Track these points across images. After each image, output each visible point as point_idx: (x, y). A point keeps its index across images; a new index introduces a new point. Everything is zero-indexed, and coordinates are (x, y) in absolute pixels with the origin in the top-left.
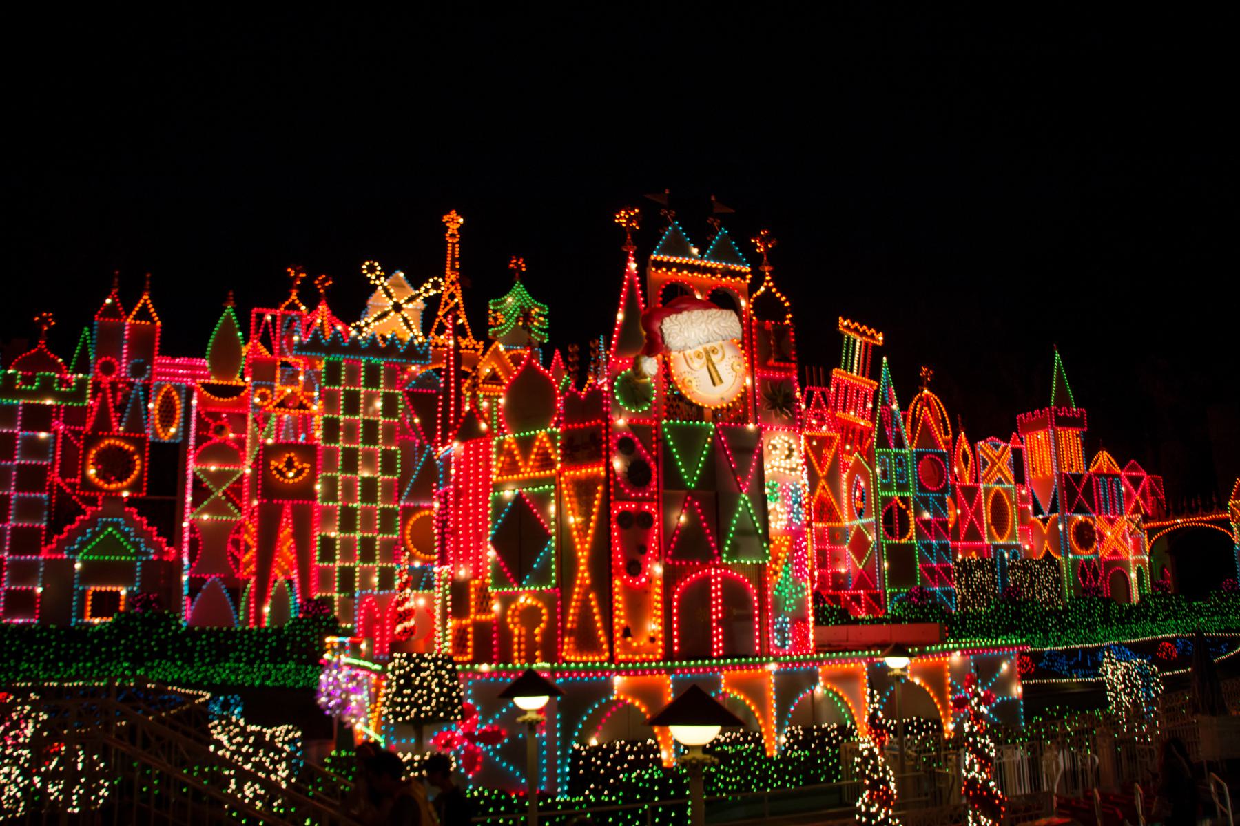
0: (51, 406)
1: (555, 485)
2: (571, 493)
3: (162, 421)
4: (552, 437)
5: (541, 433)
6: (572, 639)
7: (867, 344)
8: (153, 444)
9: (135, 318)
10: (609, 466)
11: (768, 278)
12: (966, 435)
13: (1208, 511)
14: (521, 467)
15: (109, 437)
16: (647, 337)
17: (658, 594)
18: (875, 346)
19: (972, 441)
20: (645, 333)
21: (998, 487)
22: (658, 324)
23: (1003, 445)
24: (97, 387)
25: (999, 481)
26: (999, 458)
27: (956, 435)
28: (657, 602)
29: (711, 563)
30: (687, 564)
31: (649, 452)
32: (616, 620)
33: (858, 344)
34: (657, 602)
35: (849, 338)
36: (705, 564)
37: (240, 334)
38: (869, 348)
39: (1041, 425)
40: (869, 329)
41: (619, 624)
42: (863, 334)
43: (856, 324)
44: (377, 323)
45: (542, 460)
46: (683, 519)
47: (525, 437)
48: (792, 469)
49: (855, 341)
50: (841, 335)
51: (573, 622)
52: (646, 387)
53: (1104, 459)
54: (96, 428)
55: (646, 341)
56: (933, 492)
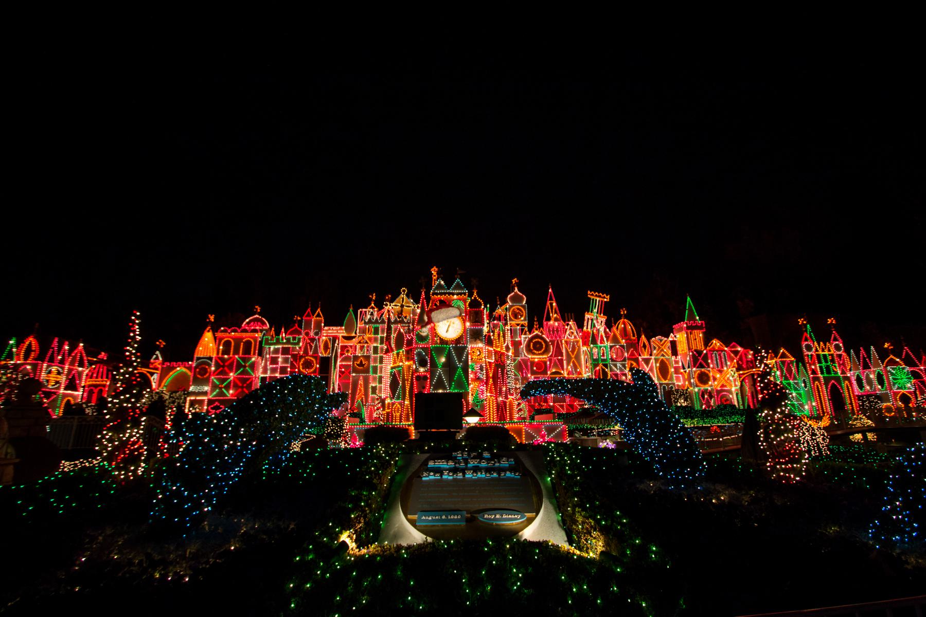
4: (403, 351)
5: (401, 351)
7: (602, 301)
9: (316, 317)
11: (475, 294)
12: (645, 336)
18: (606, 302)
19: (649, 339)
21: (662, 357)
23: (666, 339)
25: (663, 355)
26: (662, 345)
27: (639, 337)
33: (597, 302)
35: (593, 299)
38: (603, 303)
39: (680, 330)
40: (603, 295)
42: (600, 296)
43: (597, 293)
48: (480, 359)
49: (596, 300)
50: (590, 299)
53: (716, 343)
56: (618, 361)
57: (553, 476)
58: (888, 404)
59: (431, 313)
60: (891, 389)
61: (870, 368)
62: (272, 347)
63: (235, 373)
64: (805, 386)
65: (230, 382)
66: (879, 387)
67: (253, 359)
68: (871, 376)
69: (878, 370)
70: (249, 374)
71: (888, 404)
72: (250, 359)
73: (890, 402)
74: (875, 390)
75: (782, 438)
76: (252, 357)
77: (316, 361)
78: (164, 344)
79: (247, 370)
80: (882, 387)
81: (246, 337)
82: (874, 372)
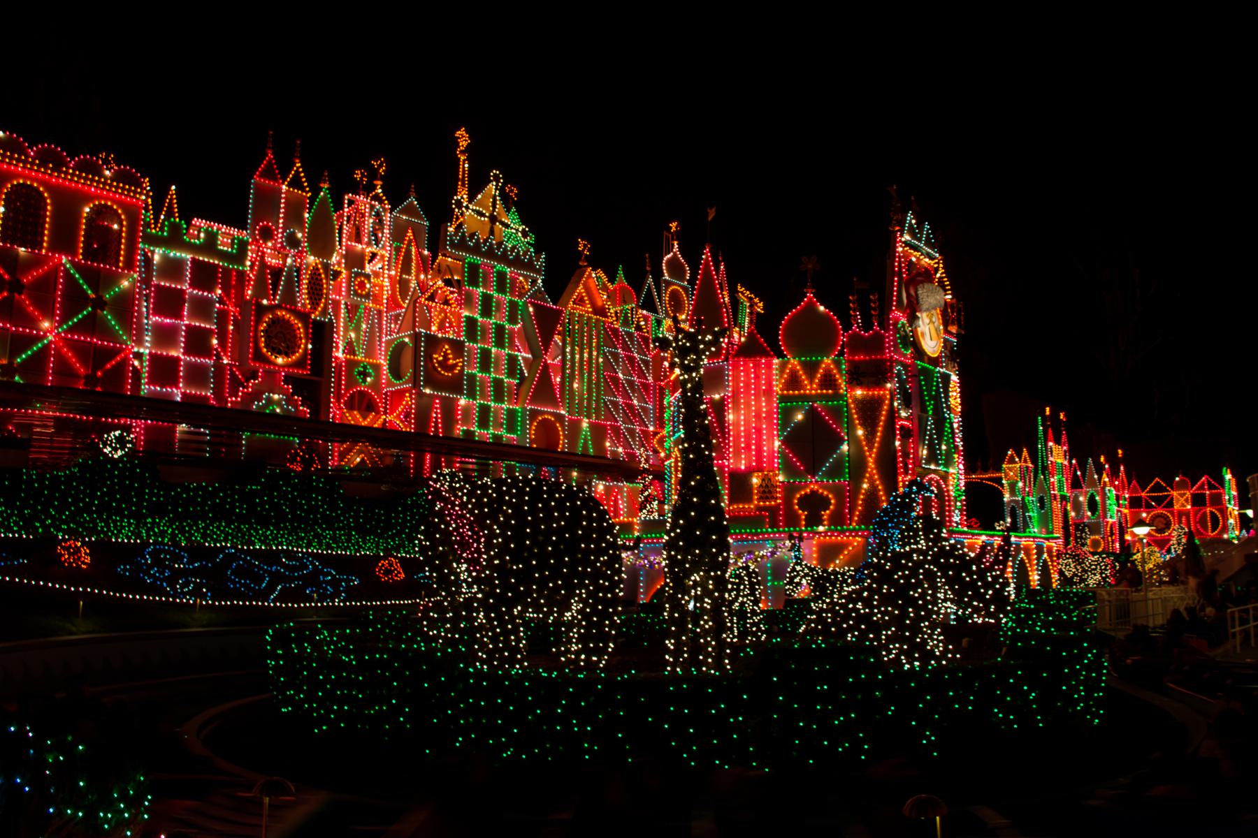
13: (986, 471)
14: (806, 385)
45: (825, 381)
47: (811, 361)
57: (686, 655)
58: (1097, 537)
60: (1105, 517)
61: (1082, 488)
62: (158, 255)
63: (60, 323)
64: (1042, 507)
65: (46, 348)
66: (1089, 513)
67: (125, 284)
68: (1081, 499)
69: (1091, 491)
70: (108, 333)
71: (1097, 537)
72: (114, 279)
73: (1100, 534)
74: (1083, 518)
76: (122, 276)
77: (306, 327)
79: (105, 322)
80: (1093, 514)
82: (1086, 493)
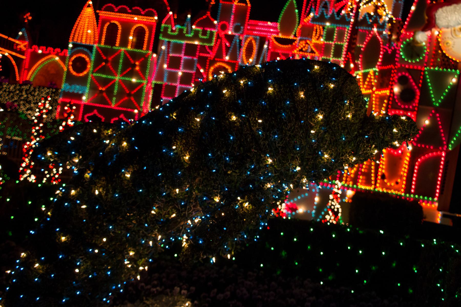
0: (197, 45)
1: (370, 99)
2: (378, 103)
3: (246, 56)
6: (364, 177)
8: (241, 67)
10: (391, 90)
15: (220, 61)
16: (428, 20)
17: (407, 160)
20: (426, 17)
22: (434, 13)
24: (218, 37)
28: (406, 164)
29: (440, 148)
30: (425, 147)
31: (417, 84)
32: (380, 170)
34: (406, 164)
36: (436, 149)
37: (297, 11)
41: (381, 172)
44: (365, 6)
46: (427, 122)
51: (365, 169)
52: (421, 48)
54: (216, 57)
55: (426, 22)
59: (436, 9)
75: (418, 60)
78: (28, 14)
81: (138, 22)
